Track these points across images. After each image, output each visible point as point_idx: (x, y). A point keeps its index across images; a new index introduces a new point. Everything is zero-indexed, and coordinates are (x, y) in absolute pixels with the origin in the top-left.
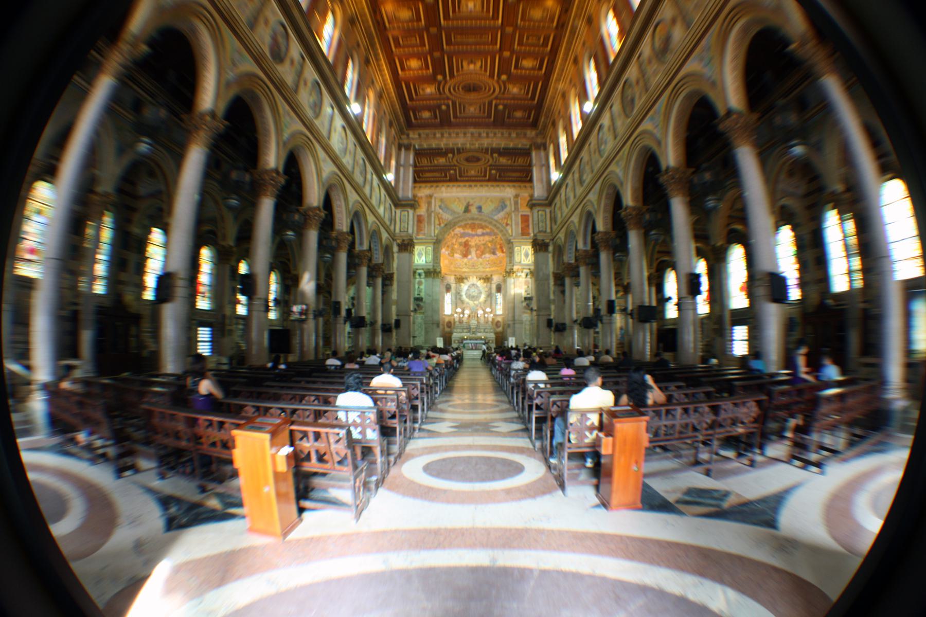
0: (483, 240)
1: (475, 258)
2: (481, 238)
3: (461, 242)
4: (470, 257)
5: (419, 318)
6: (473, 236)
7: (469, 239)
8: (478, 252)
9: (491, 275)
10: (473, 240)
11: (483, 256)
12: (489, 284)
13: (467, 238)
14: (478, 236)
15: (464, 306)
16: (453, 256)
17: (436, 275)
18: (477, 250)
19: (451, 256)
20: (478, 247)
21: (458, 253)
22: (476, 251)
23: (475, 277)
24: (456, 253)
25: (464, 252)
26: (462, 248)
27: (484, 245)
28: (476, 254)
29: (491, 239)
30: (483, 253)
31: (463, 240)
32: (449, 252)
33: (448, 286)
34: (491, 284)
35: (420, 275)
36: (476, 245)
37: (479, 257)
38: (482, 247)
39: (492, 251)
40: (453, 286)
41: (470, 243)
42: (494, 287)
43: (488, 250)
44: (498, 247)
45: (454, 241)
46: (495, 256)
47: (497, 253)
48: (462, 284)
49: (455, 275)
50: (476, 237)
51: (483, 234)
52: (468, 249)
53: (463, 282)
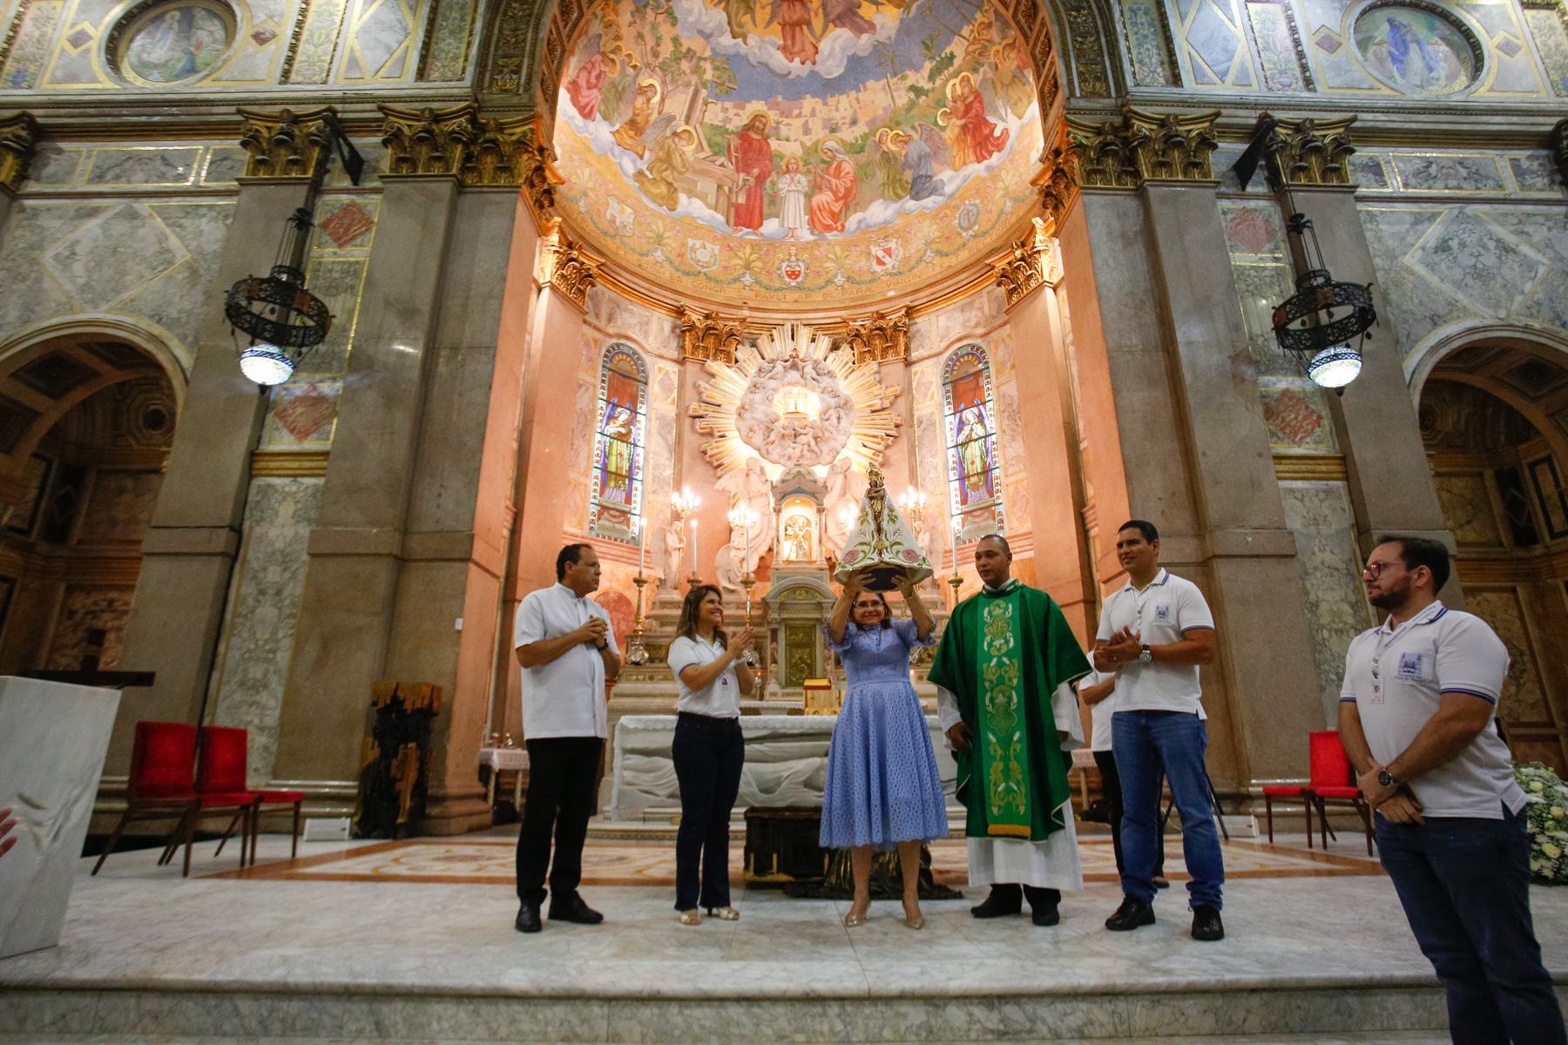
0: (854, 122)
1: (806, 235)
2: (843, 105)
3: (720, 130)
4: (770, 226)
5: (286, 510)
6: (794, 89)
7: (773, 115)
8: (824, 197)
9: (910, 312)
10: (791, 128)
11: (852, 221)
12: (895, 369)
13: (756, 106)
14: (828, 88)
15: (727, 482)
16: (670, 201)
17: (490, 161)
18: (816, 187)
19: (654, 198)
20: (819, 166)
21: (703, 198)
22: (808, 197)
23: (804, 334)
24: (691, 193)
25: (742, 200)
26: (725, 168)
27: (855, 149)
28: (811, 211)
29: (903, 98)
30: (849, 200)
31: (739, 120)
32: (643, 166)
33: (625, 365)
34: (908, 363)
35: (356, 167)
36: (810, 152)
37: (829, 228)
38: (848, 167)
39: (909, 175)
40: (662, 374)
41: (774, 144)
42: (929, 377)
43: (881, 176)
44: (951, 129)
45: (677, 105)
46: (930, 202)
47: (945, 175)
48: (716, 366)
49: (680, 312)
50: (809, 103)
51: (857, 71)
52: (760, 180)
53: (731, 360)
